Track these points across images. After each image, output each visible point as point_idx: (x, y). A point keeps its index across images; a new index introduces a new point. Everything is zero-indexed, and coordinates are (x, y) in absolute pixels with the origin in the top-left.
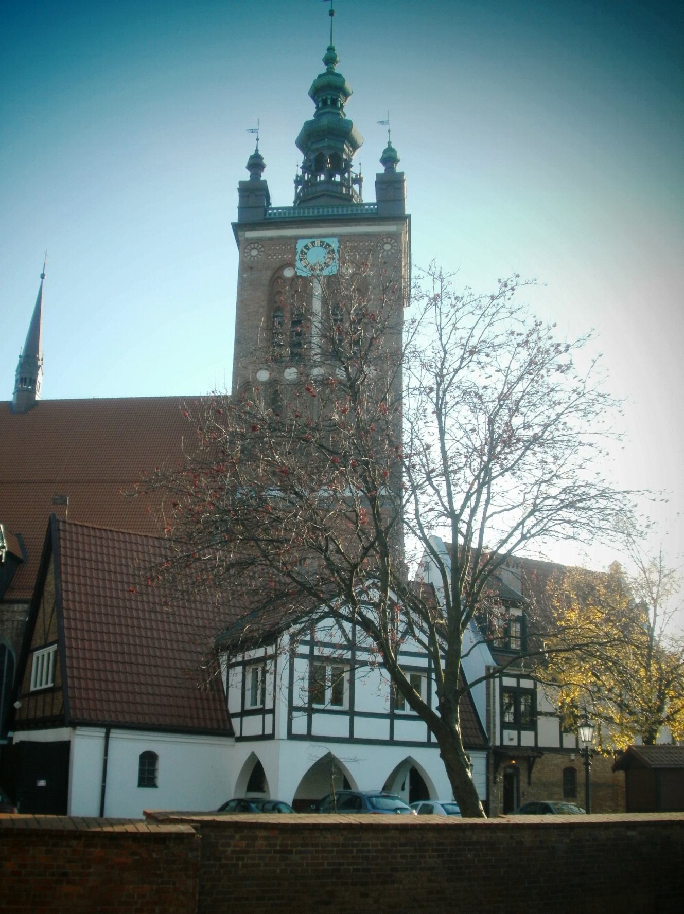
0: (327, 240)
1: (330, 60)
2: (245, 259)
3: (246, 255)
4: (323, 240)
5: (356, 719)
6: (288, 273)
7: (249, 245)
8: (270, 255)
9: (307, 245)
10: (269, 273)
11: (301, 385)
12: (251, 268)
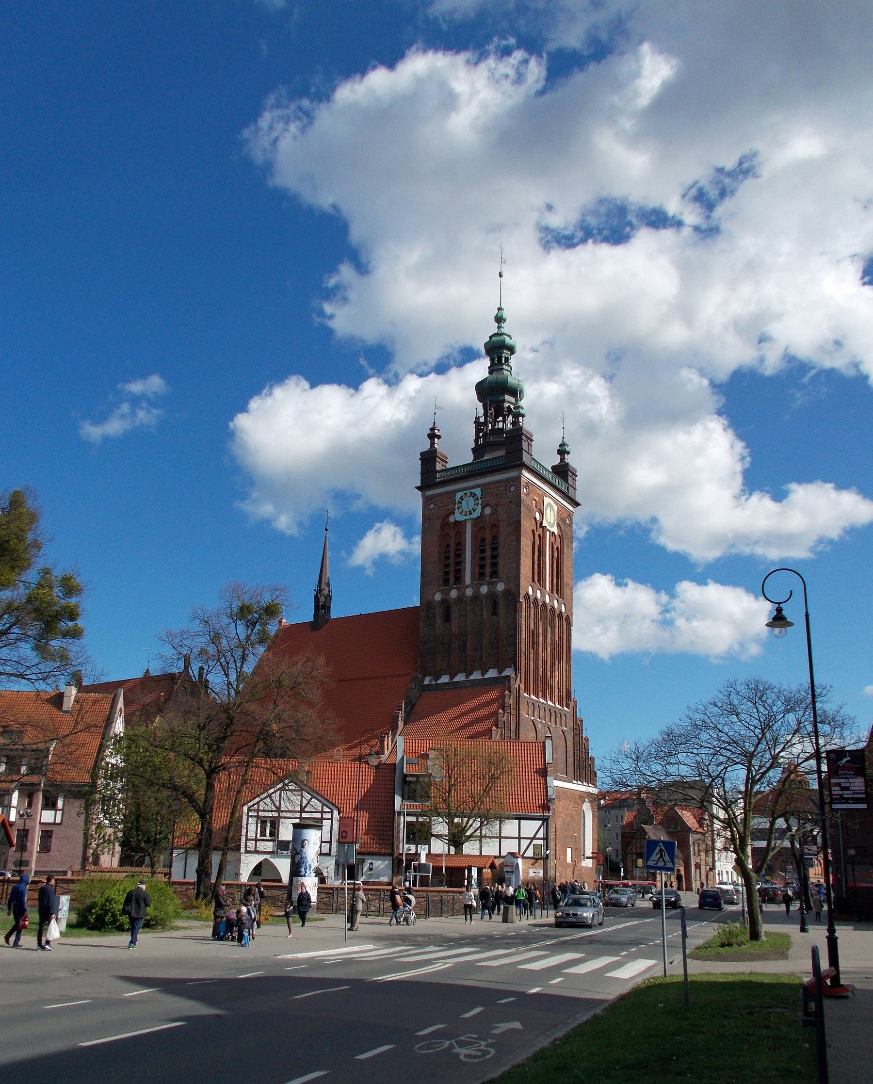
4: (472, 491)
6: (452, 519)
9: (462, 497)
10: (440, 521)
11: (460, 599)
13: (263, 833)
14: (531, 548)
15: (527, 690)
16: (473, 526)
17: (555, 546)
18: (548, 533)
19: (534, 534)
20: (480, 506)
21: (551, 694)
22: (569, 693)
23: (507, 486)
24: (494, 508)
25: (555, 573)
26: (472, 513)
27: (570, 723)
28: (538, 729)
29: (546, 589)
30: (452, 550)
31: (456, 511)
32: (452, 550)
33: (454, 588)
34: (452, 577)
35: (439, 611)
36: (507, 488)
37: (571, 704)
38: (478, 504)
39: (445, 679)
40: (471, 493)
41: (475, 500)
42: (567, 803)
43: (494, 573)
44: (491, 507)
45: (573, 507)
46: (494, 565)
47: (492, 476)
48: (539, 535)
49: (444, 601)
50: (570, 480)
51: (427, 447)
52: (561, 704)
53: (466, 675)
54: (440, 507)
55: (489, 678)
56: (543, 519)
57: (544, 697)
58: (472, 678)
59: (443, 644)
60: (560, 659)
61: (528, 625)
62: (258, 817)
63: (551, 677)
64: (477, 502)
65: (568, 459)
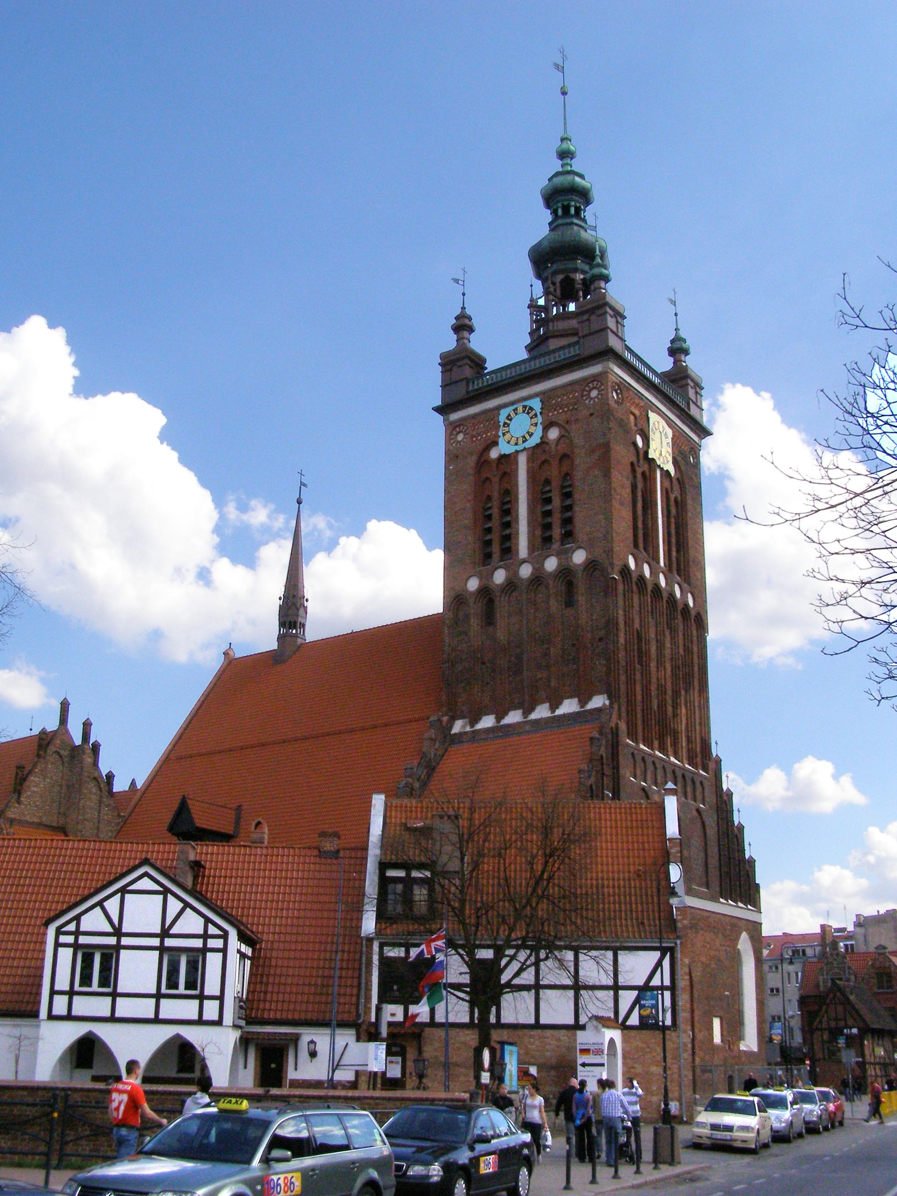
0: (528, 403)
1: (564, 155)
2: (451, 448)
3: (452, 441)
5: (153, 1000)
6: (494, 454)
7: (453, 430)
8: (474, 436)
9: (509, 415)
10: (474, 458)
11: (511, 585)
12: (457, 457)
13: (86, 979)
14: (629, 490)
15: (632, 735)
16: (530, 460)
17: (672, 497)
19: (634, 471)
20: (540, 428)
21: (675, 744)
23: (584, 390)
24: (564, 428)
25: (673, 540)
26: (526, 440)
27: (711, 798)
29: (658, 562)
31: (501, 440)
33: (500, 567)
34: (496, 548)
35: (475, 609)
36: (585, 393)
37: (711, 765)
38: (536, 425)
39: (487, 722)
40: (525, 407)
41: (532, 418)
42: (709, 936)
43: (568, 535)
45: (699, 436)
47: (558, 376)
48: (643, 474)
49: (485, 592)
51: (450, 342)
53: (524, 713)
54: (474, 436)
55: (564, 715)
56: (648, 447)
57: (662, 749)
58: (533, 716)
59: (484, 663)
60: (688, 687)
61: (628, 622)
62: (76, 946)
63: (675, 715)
64: (534, 420)
65: (691, 362)
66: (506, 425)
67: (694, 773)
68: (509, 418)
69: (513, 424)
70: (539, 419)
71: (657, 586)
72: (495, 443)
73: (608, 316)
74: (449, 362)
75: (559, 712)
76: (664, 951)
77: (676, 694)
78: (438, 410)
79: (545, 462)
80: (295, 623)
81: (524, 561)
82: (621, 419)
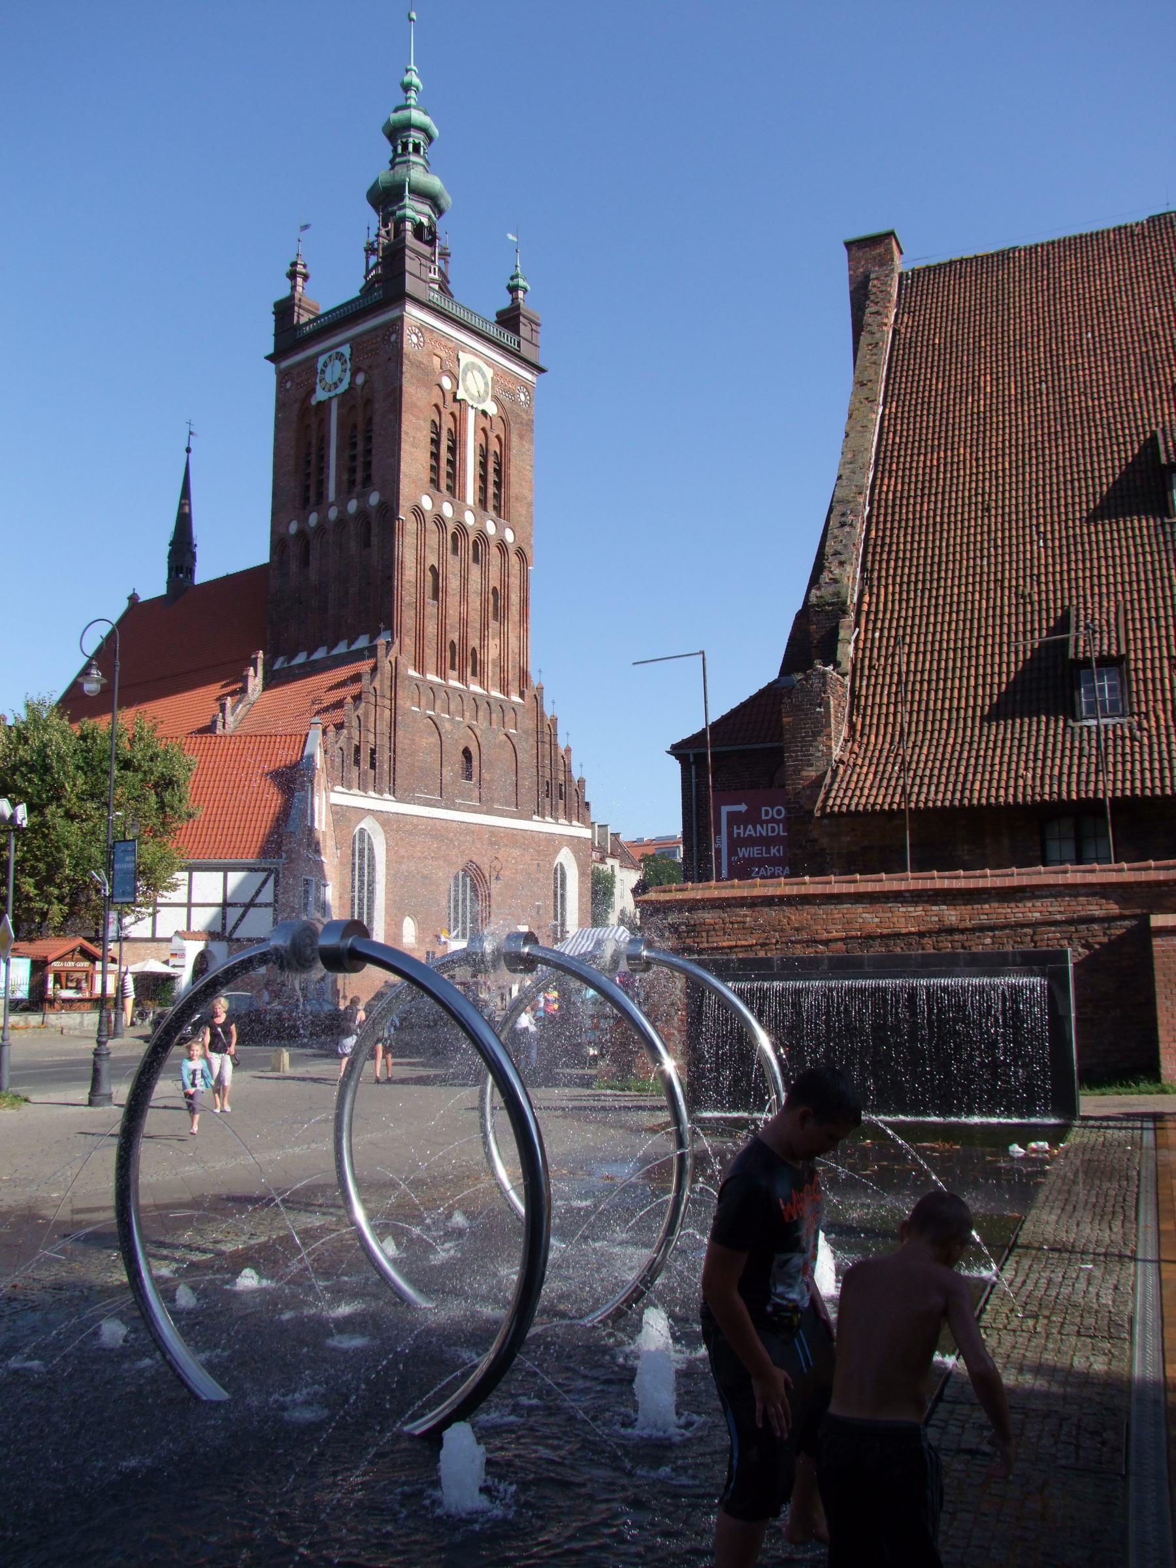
4: (340, 350)
6: (314, 402)
10: (297, 406)
11: (321, 528)
15: (420, 666)
16: (340, 406)
17: (492, 436)
18: (471, 414)
20: (348, 374)
22: (524, 676)
28: (442, 731)
29: (464, 501)
30: (314, 450)
31: (318, 388)
32: (314, 450)
39: (301, 659)
42: (516, 852)
43: (368, 479)
44: (366, 372)
46: (368, 465)
49: (301, 533)
50: (524, 330)
52: (504, 690)
58: (335, 652)
61: (420, 560)
63: (482, 647)
66: (323, 372)
67: (501, 700)
68: (325, 365)
69: (328, 370)
70: (349, 365)
71: (461, 527)
72: (313, 391)
73: (407, 259)
74: (284, 310)
75: (353, 648)
76: (269, 871)
77: (484, 626)
78: (270, 358)
79: (353, 407)
80: (182, 568)
81: (332, 505)
82: (420, 362)
